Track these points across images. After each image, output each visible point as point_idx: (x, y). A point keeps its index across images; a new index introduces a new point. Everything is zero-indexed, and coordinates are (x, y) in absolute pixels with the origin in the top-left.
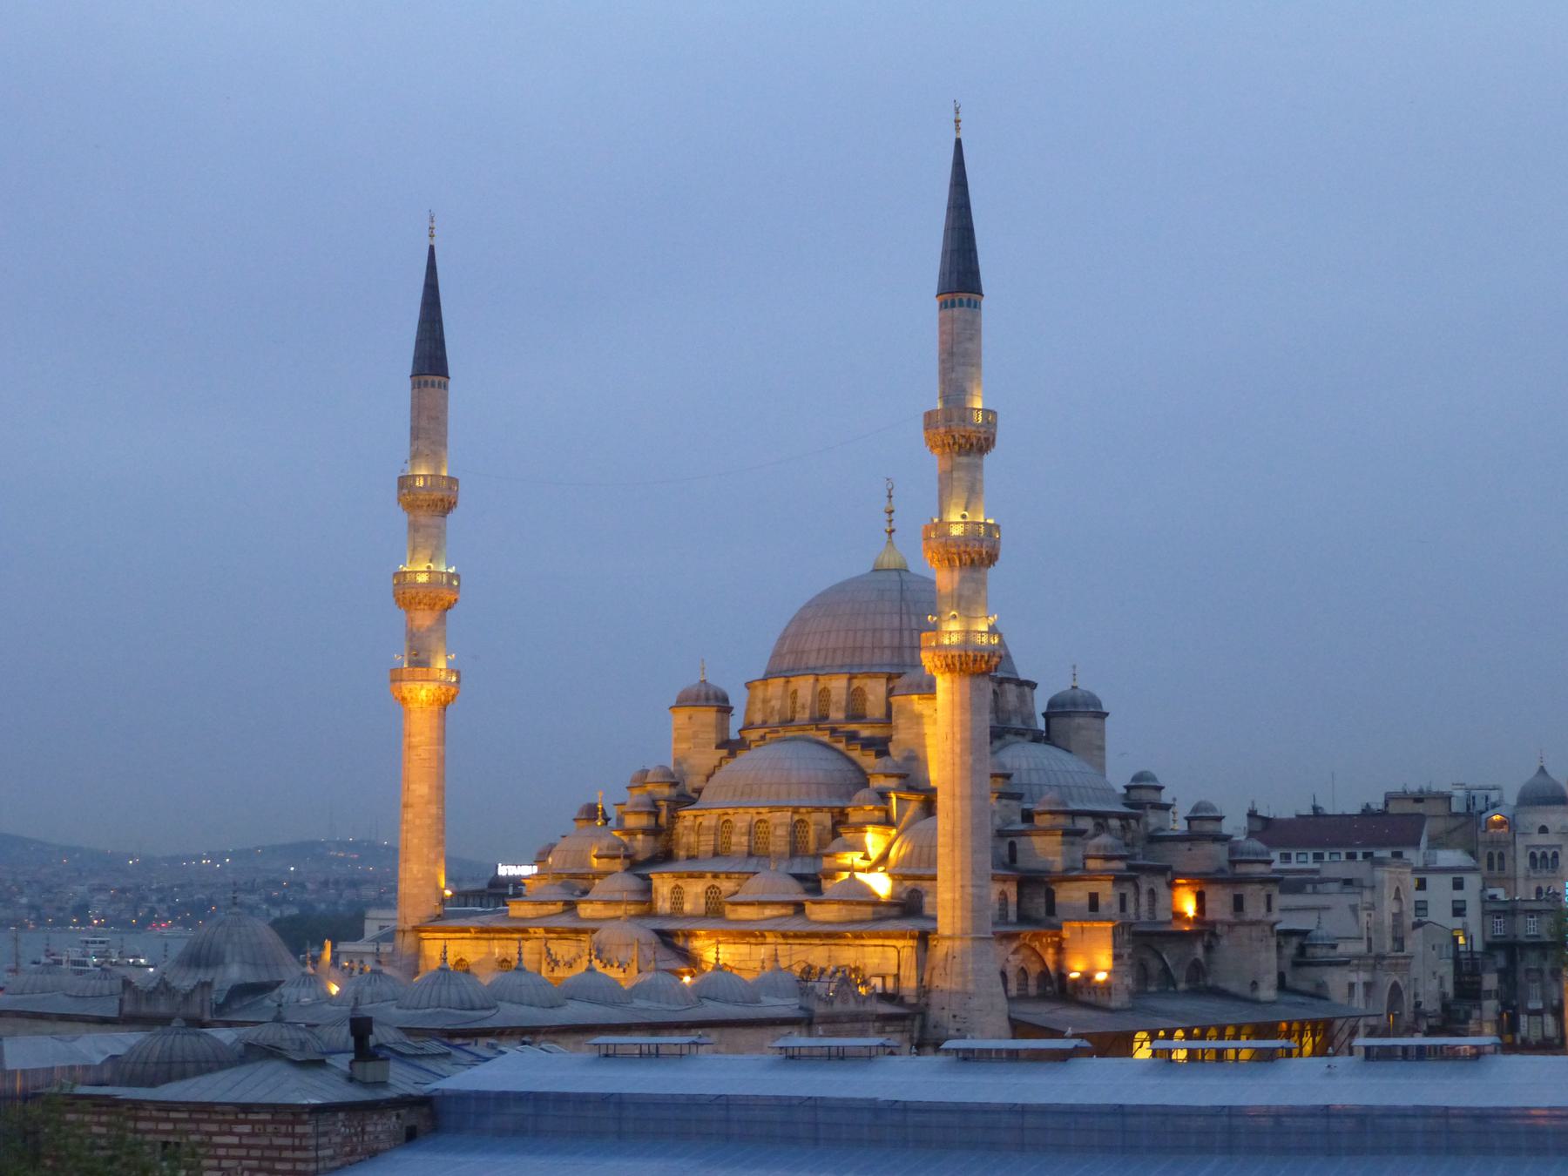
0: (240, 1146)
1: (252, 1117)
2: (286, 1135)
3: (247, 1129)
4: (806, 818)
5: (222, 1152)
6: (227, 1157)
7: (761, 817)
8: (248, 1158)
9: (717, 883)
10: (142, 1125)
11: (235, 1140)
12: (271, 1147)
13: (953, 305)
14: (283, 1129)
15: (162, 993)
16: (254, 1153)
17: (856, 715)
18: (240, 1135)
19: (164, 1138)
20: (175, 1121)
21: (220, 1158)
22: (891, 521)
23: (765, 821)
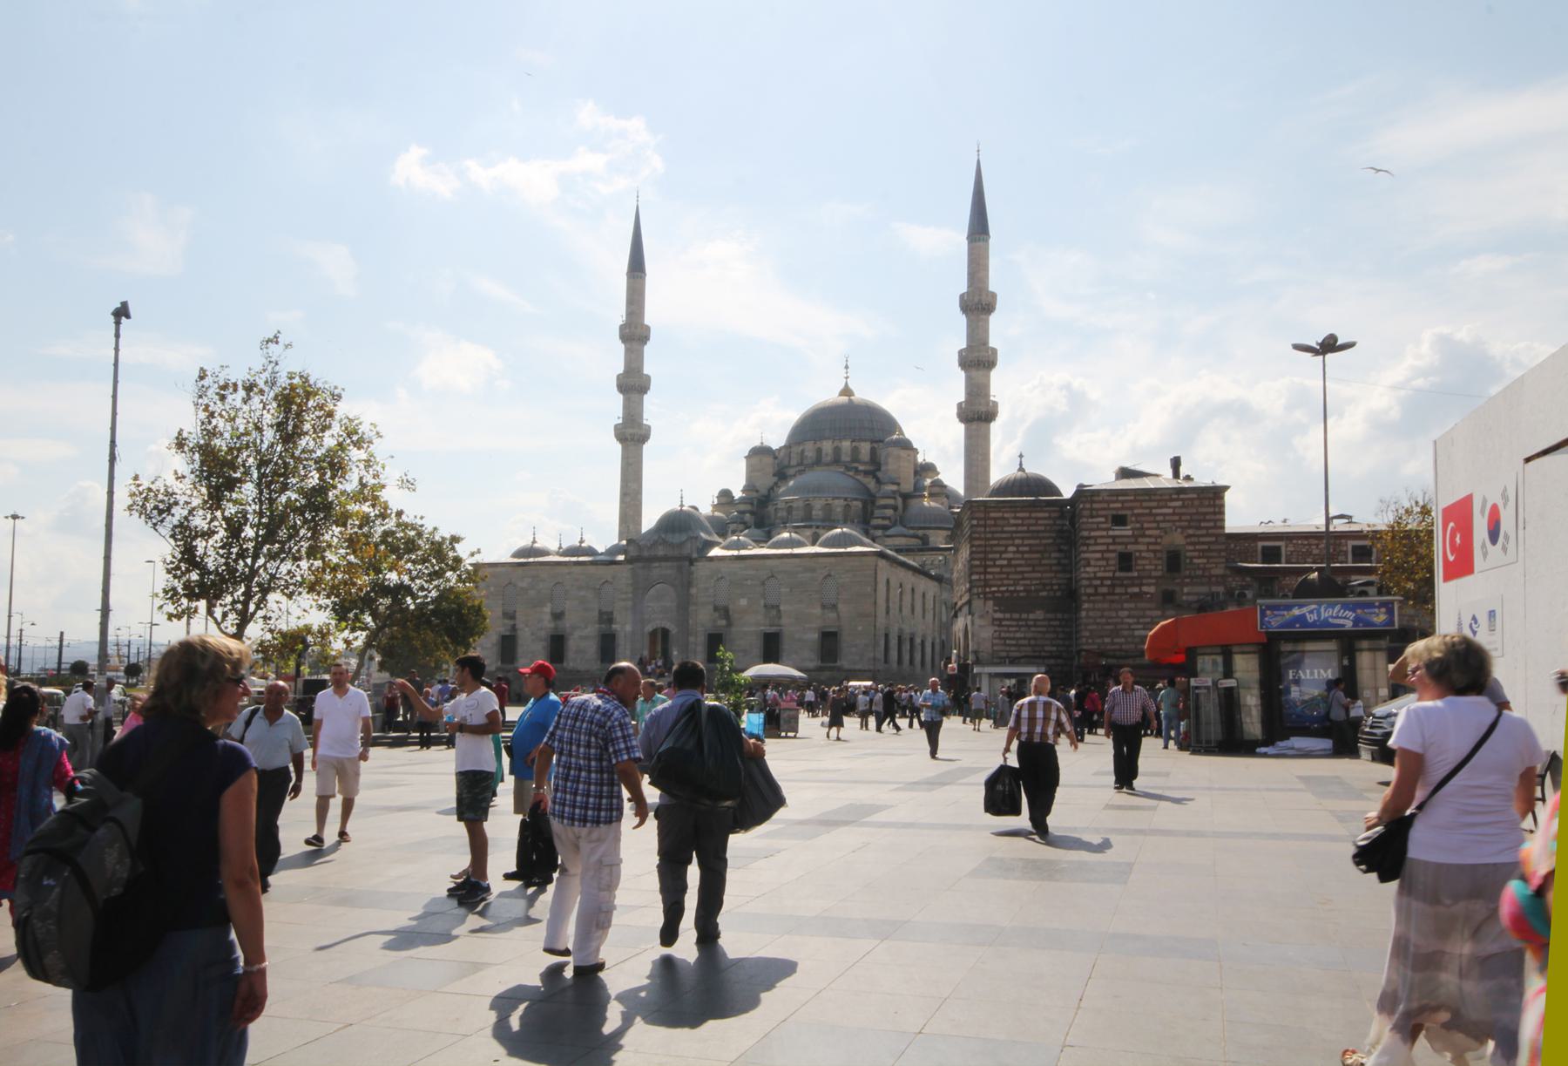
0: (1174, 514)
1: (1182, 496)
2: (1209, 506)
3: (1179, 503)
4: (850, 503)
5: (1159, 518)
6: (1164, 521)
8: (1180, 520)
9: (817, 530)
10: (1095, 506)
11: (1171, 511)
12: (1197, 513)
13: (979, 240)
14: (1207, 503)
15: (660, 544)
16: (1184, 518)
18: (1174, 508)
19: (1114, 512)
20: (1123, 502)
21: (1158, 522)
22: (847, 373)
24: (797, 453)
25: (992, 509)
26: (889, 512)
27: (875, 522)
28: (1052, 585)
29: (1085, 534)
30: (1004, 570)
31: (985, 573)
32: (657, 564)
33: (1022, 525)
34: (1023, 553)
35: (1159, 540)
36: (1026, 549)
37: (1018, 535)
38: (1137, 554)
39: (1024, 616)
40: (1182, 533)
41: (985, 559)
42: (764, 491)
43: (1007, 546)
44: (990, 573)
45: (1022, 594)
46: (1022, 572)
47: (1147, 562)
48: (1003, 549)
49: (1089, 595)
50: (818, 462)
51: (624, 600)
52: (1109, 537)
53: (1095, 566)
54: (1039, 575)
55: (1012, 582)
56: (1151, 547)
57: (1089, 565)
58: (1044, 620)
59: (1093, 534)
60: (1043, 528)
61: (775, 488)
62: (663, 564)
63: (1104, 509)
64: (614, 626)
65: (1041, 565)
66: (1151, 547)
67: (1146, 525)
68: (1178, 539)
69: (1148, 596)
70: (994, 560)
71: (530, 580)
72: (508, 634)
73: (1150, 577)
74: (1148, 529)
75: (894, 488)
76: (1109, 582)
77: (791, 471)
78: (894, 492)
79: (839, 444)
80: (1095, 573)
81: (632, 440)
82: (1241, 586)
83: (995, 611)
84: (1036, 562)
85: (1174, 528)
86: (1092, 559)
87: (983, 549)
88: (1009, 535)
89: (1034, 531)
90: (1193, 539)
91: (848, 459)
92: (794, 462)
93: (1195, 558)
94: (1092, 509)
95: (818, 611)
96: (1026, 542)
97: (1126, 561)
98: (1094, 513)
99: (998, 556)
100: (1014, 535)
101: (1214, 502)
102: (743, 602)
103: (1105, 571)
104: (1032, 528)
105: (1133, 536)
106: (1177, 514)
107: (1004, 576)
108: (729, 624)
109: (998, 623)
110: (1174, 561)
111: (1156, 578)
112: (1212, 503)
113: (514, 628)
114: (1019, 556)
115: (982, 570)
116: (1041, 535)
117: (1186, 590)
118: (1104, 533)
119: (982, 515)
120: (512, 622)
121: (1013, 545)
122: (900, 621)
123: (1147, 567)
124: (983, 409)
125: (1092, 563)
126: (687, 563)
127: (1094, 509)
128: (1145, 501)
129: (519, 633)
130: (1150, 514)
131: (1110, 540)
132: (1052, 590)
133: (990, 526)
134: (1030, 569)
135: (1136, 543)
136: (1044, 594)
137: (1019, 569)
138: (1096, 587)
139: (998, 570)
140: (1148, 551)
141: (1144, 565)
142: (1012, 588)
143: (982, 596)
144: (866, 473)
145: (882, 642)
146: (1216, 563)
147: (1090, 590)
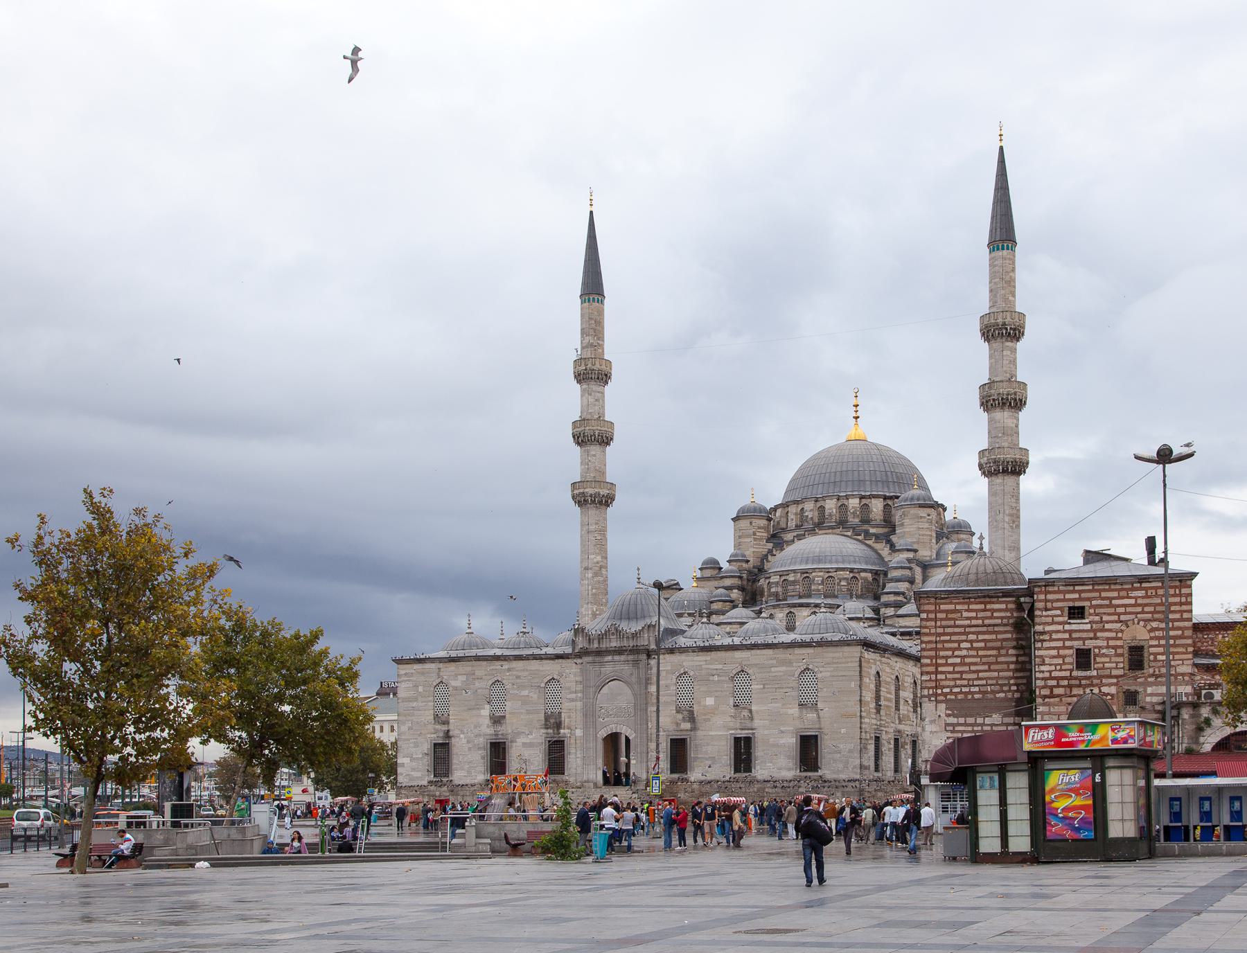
0: (1136, 605)
1: (1144, 585)
2: (1174, 595)
3: (1141, 593)
4: (857, 575)
6: (1125, 613)
7: (830, 574)
8: (1143, 612)
10: (1050, 597)
11: (1132, 601)
14: (1172, 591)
15: (613, 634)
16: (1146, 609)
17: (865, 521)
18: (1136, 598)
19: (1071, 604)
20: (1080, 592)
21: (1119, 614)
23: (831, 577)
24: (796, 514)
25: (942, 601)
26: (903, 586)
27: (884, 599)
28: (1010, 685)
29: (1039, 628)
30: (957, 669)
31: (937, 672)
32: (610, 658)
33: (976, 618)
34: (977, 649)
35: (1120, 635)
36: (982, 645)
37: (973, 629)
38: (1097, 650)
39: (980, 720)
40: (1145, 627)
41: (937, 657)
42: (753, 561)
43: (959, 642)
44: (942, 673)
45: (976, 696)
46: (978, 672)
47: (1108, 660)
48: (956, 645)
49: (1045, 697)
50: (820, 525)
51: (572, 700)
52: (1065, 631)
53: (1050, 665)
54: (996, 674)
55: (965, 682)
56: (1111, 643)
57: (1043, 664)
58: (1003, 724)
59: (1048, 628)
60: (999, 621)
61: (769, 556)
62: (617, 658)
63: (1058, 600)
64: (562, 731)
65: (997, 663)
66: (1111, 643)
67: (1105, 618)
68: (1140, 633)
69: (1109, 697)
70: (947, 657)
71: (464, 678)
72: (441, 742)
73: (1110, 676)
74: (1107, 622)
75: (911, 555)
76: (1065, 683)
77: (789, 537)
78: (909, 560)
79: (845, 502)
80: (1050, 672)
81: (593, 502)
82: (1210, 685)
83: (948, 715)
84: (992, 660)
85: (1136, 620)
86: (1046, 657)
87: (934, 646)
88: (962, 630)
89: (989, 625)
90: (1157, 633)
91: (857, 520)
92: (792, 524)
93: (1159, 654)
94: (1046, 601)
95: (794, 711)
96: (981, 637)
97: (1084, 658)
98: (1049, 605)
99: (950, 653)
100: (967, 630)
101: (1180, 591)
102: (710, 701)
103: (1061, 670)
104: (987, 622)
105: (1092, 630)
106: (1139, 605)
107: (958, 676)
108: (694, 729)
109: (951, 728)
110: (1136, 658)
111: (1116, 677)
112: (1177, 592)
113: (447, 735)
114: (973, 653)
115: (932, 669)
116: (996, 629)
117: (1149, 690)
118: (1060, 627)
119: (932, 608)
120: (445, 728)
121: (966, 641)
122: (897, 722)
123: (1107, 665)
124: (1010, 456)
125: (1047, 660)
126: (644, 657)
127: (1049, 601)
128: (1105, 590)
129: (453, 741)
130: (1110, 606)
131: (1067, 636)
132: (1010, 691)
133: (941, 620)
134: (986, 667)
135: (1096, 638)
136: (1002, 695)
137: (973, 668)
138: (1052, 688)
139: (951, 669)
140: (1108, 647)
141: (1103, 663)
142: (964, 690)
143: (933, 699)
144: (878, 537)
145: (872, 748)
146: (1183, 660)
147: (1046, 692)
